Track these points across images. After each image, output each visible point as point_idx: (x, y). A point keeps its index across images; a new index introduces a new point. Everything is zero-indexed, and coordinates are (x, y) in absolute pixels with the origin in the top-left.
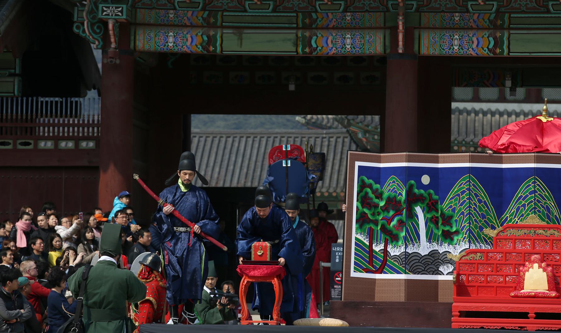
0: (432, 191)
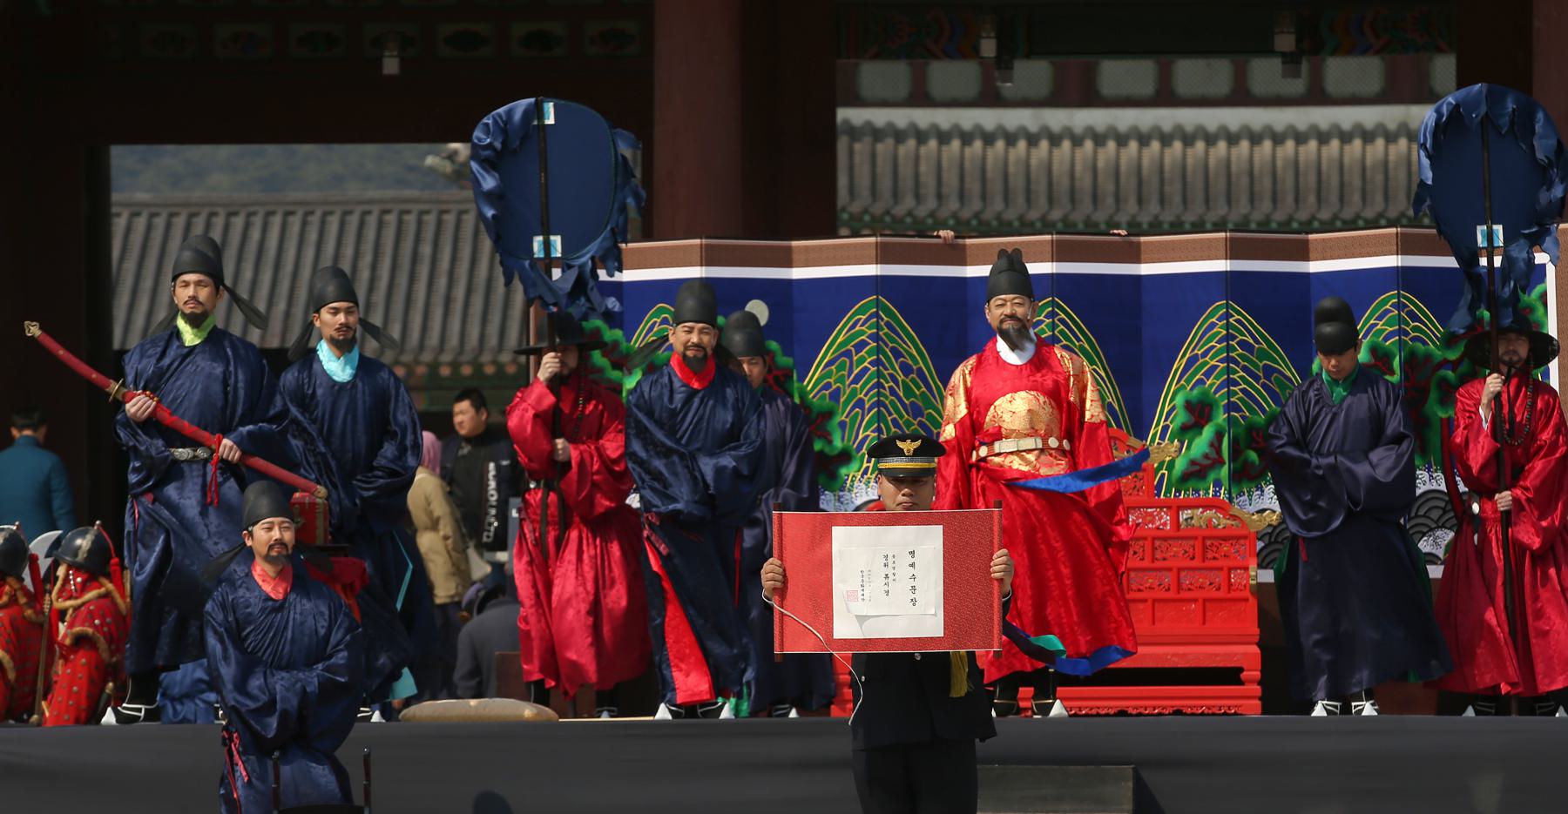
0: (773, 345)
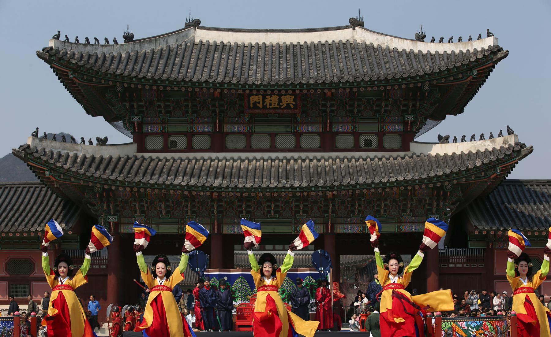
0: (228, 283)
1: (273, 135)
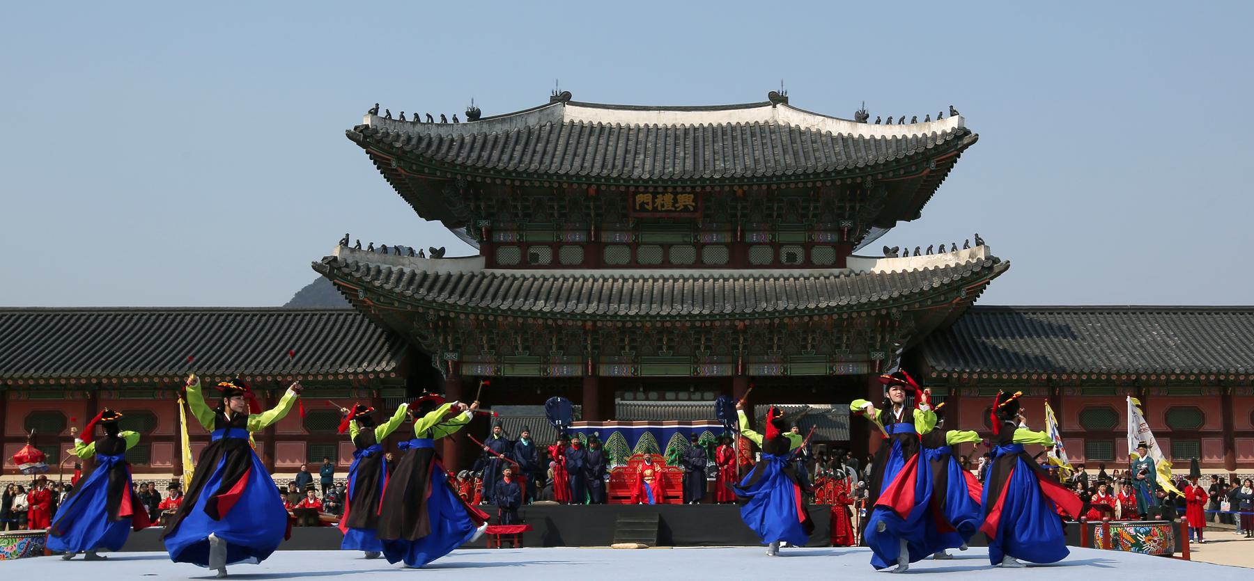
1: (666, 247)
